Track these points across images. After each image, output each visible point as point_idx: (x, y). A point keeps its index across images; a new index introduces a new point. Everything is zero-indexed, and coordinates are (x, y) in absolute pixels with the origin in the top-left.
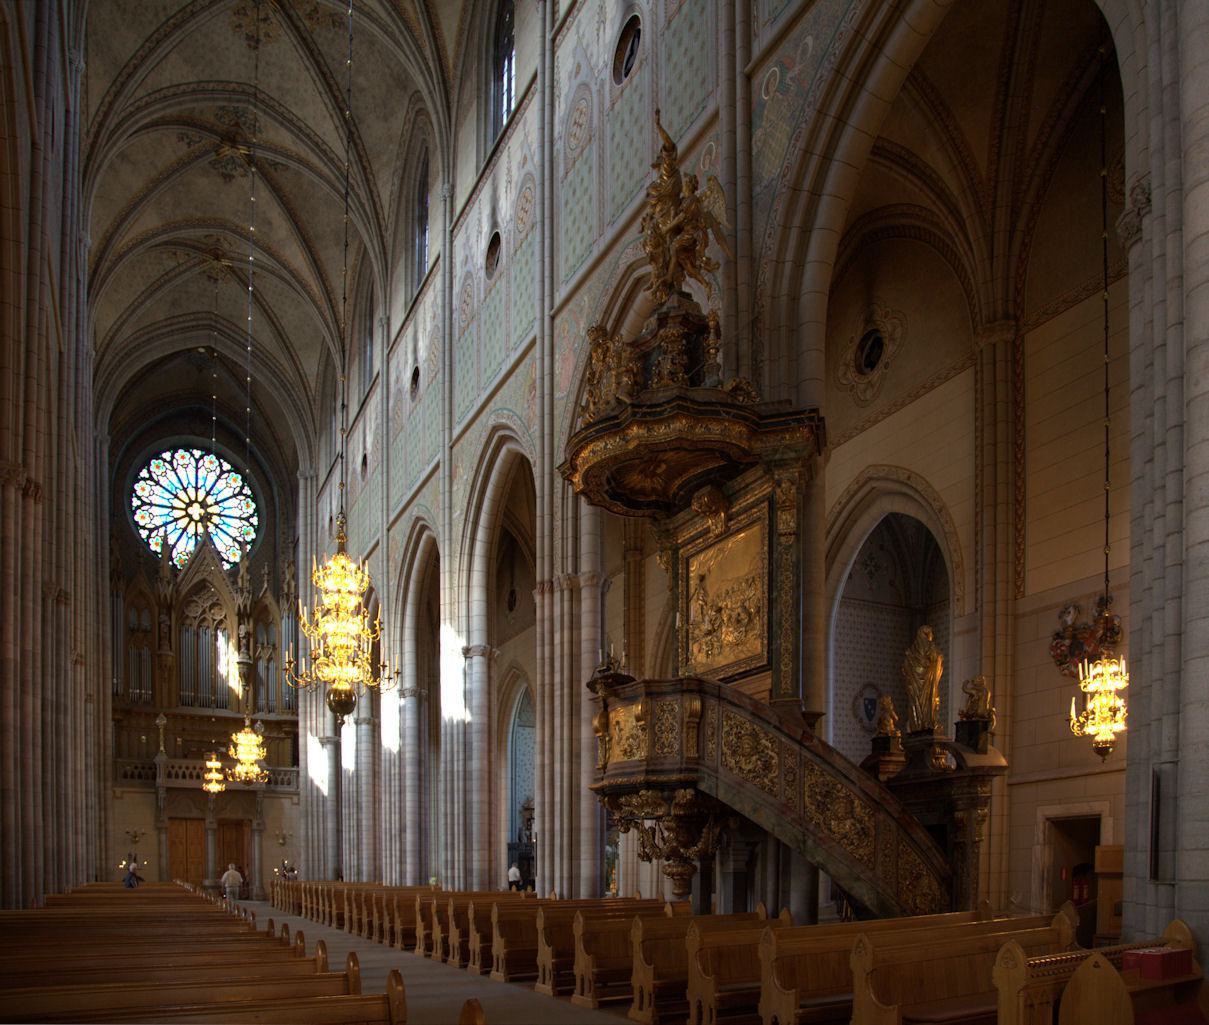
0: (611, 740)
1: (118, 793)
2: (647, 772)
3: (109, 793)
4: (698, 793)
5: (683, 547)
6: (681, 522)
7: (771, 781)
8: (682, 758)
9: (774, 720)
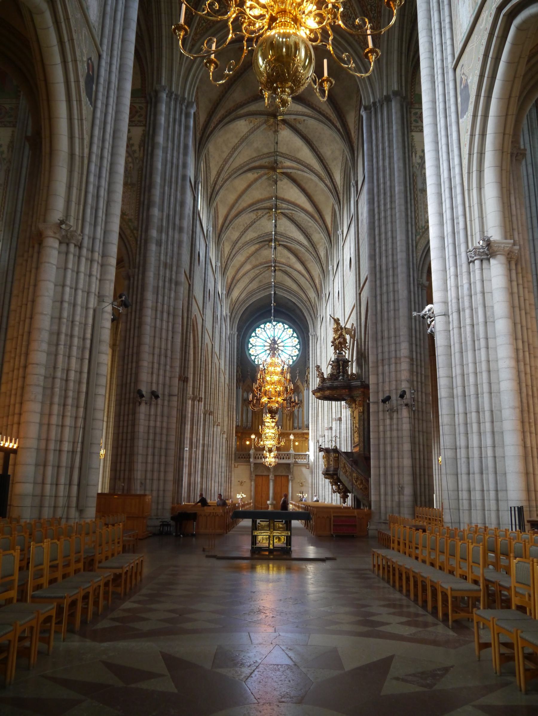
1: (236, 466)
3: (233, 466)
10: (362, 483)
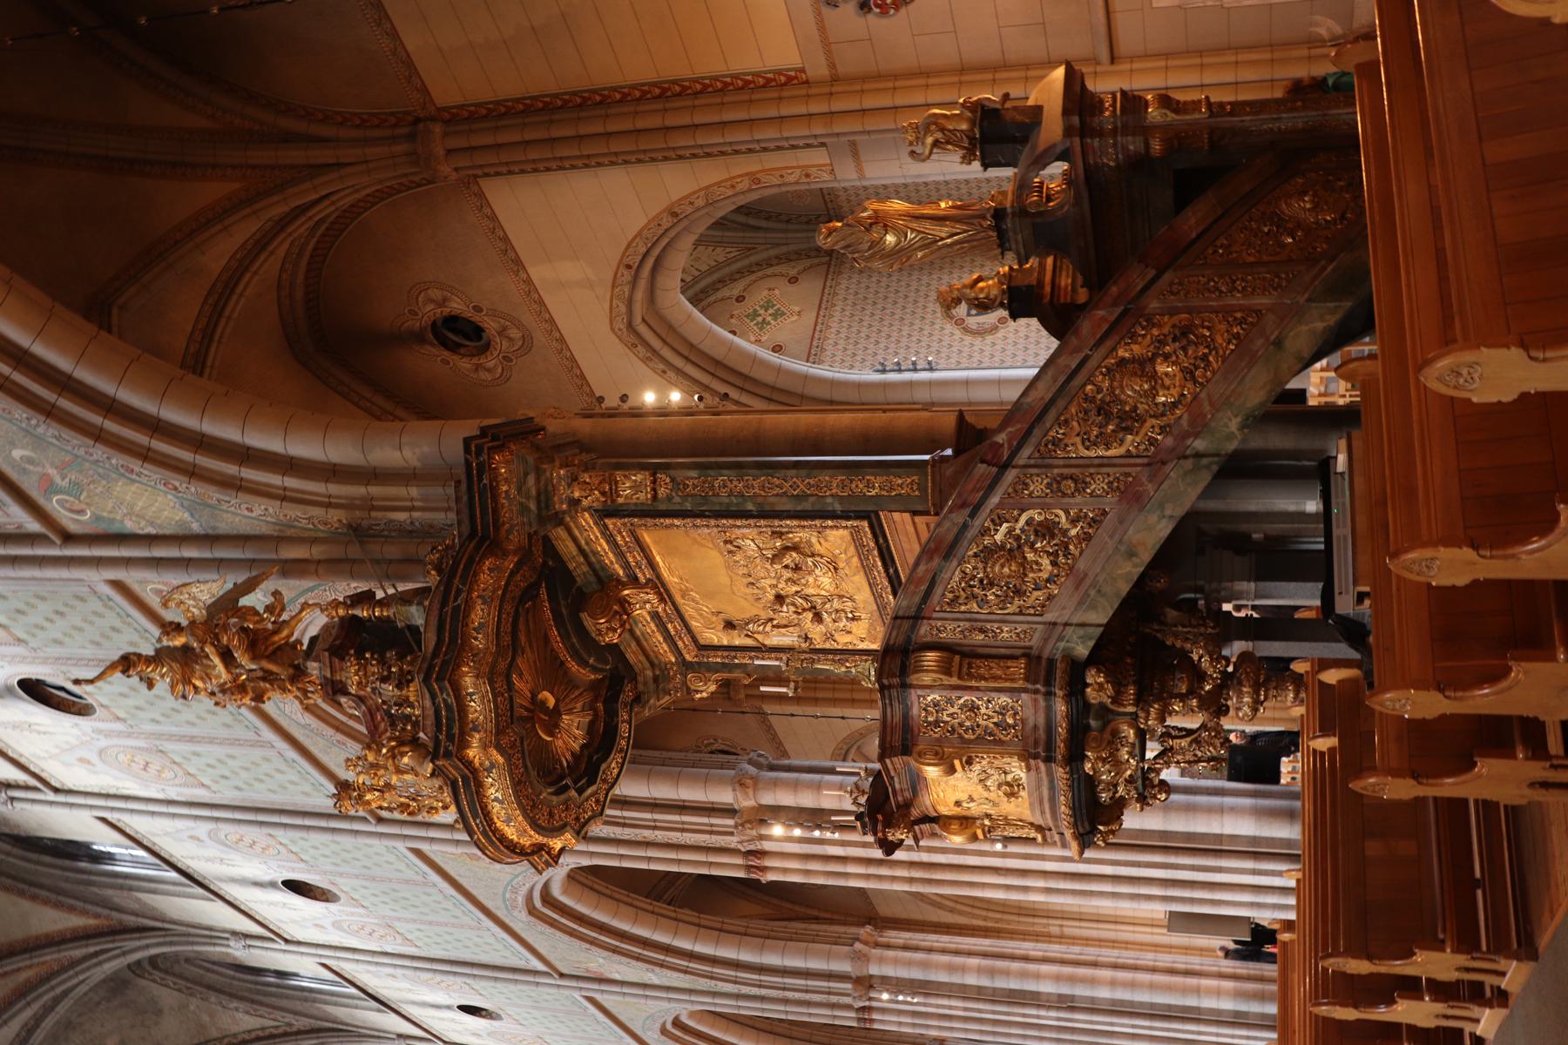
0: (988, 816)
2: (1049, 759)
4: (1094, 659)
5: (681, 654)
6: (642, 658)
7: (1074, 522)
8: (1025, 690)
9: (960, 517)
10: (1142, 367)
